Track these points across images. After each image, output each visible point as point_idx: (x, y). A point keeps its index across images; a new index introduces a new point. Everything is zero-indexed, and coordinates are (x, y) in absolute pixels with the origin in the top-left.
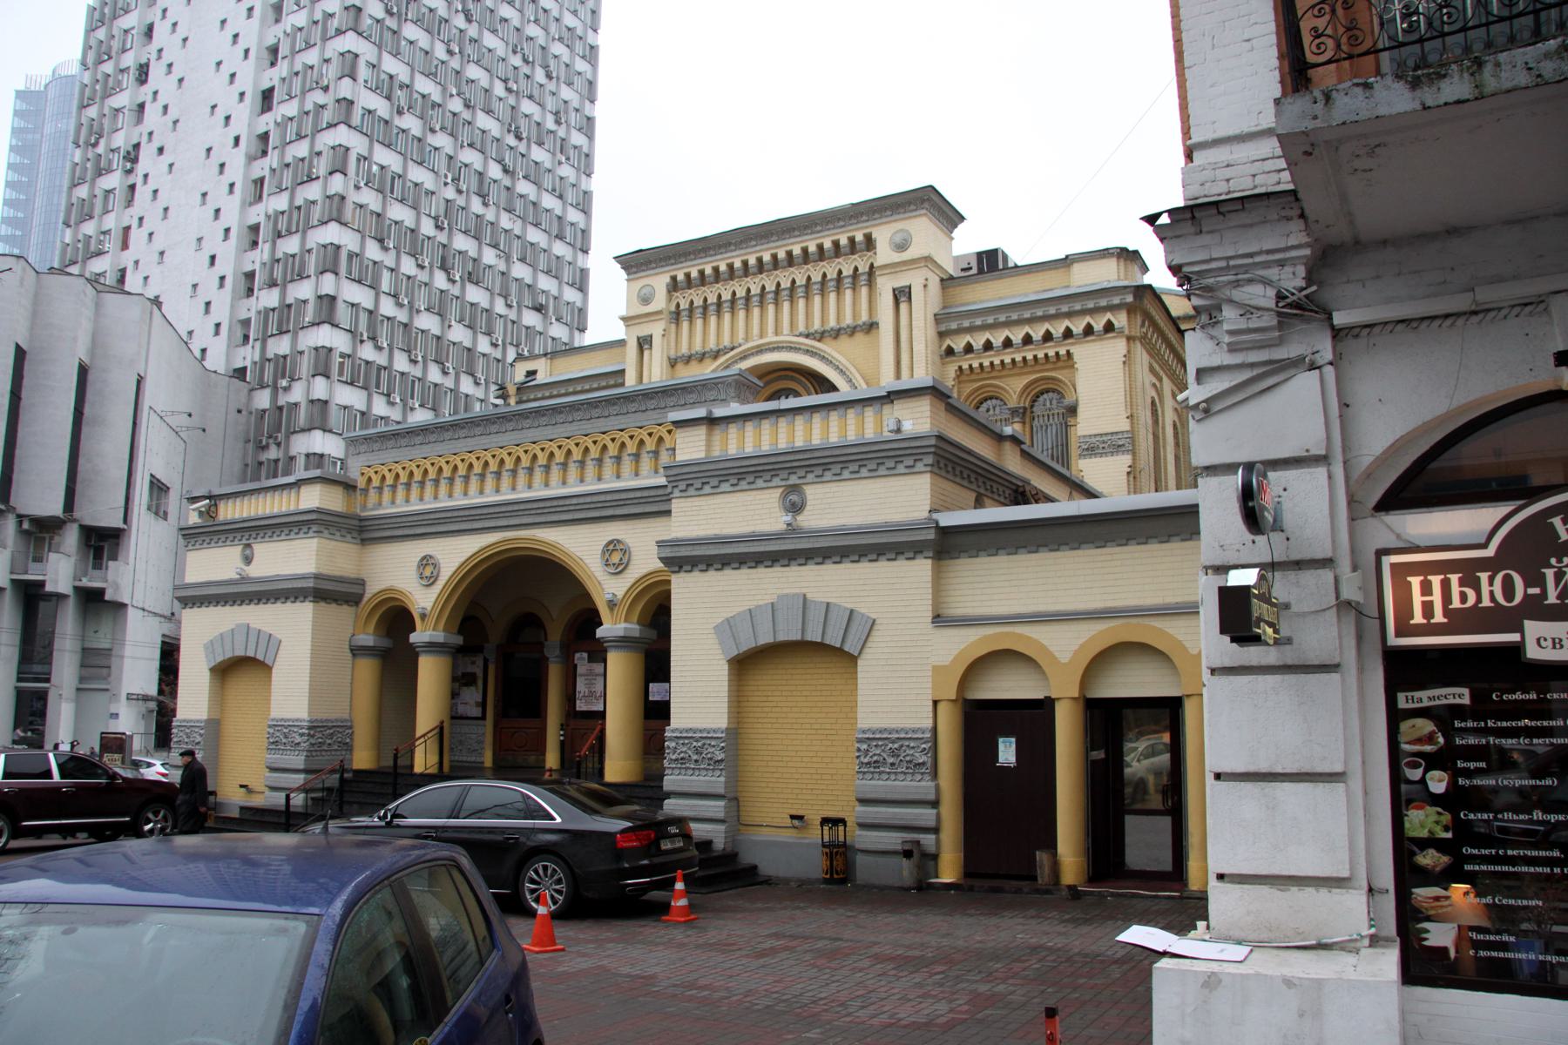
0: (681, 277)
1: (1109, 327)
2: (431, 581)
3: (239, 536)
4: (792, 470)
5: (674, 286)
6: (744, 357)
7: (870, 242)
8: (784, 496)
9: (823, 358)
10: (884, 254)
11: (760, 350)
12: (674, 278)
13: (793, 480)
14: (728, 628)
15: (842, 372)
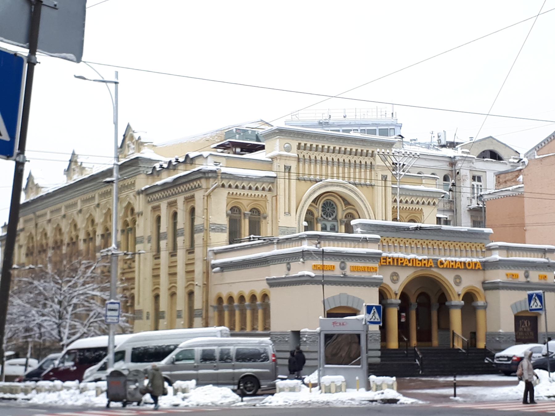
0: (303, 144)
1: (434, 204)
2: (394, 281)
3: (340, 258)
4: (528, 267)
5: (299, 147)
6: (326, 186)
7: (372, 155)
8: (525, 274)
9: (356, 194)
10: (378, 161)
11: (332, 184)
12: (299, 144)
13: (527, 269)
14: (514, 306)
15: (362, 201)
